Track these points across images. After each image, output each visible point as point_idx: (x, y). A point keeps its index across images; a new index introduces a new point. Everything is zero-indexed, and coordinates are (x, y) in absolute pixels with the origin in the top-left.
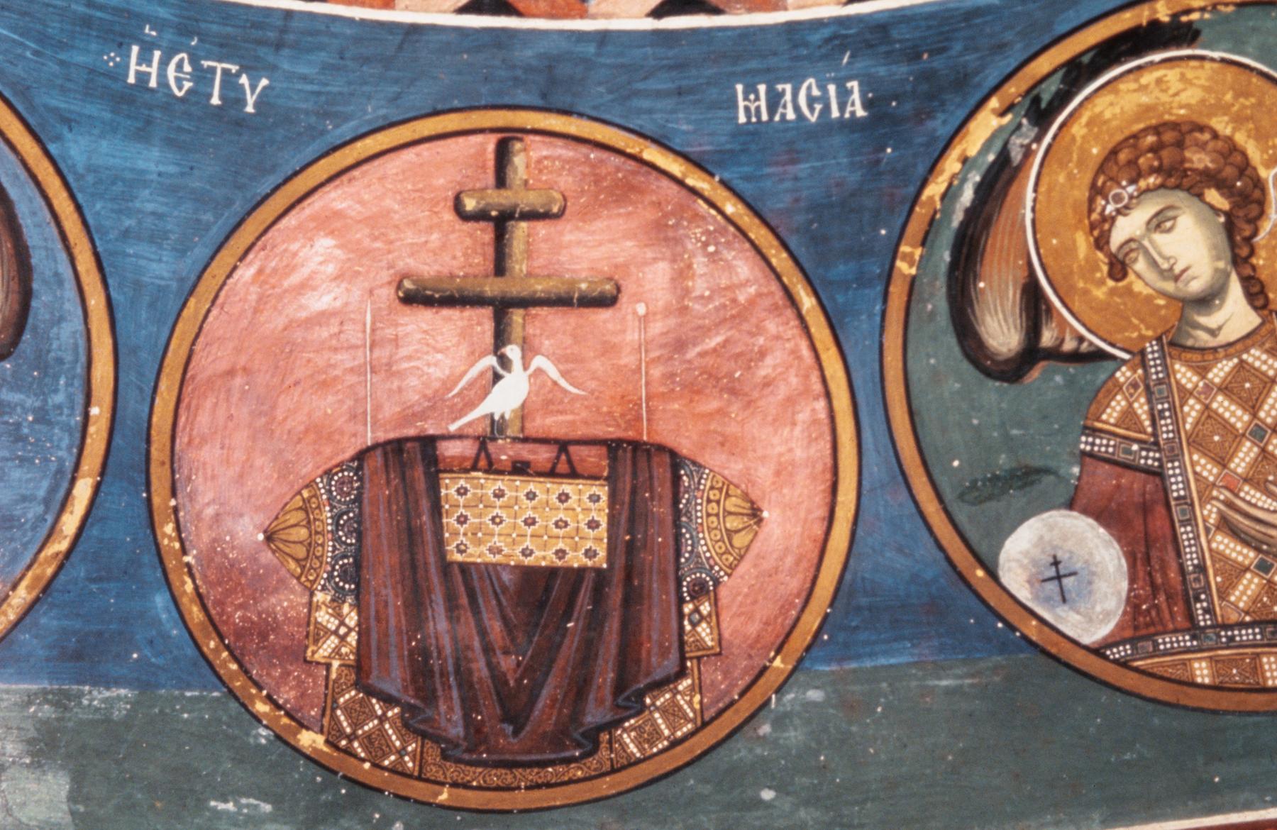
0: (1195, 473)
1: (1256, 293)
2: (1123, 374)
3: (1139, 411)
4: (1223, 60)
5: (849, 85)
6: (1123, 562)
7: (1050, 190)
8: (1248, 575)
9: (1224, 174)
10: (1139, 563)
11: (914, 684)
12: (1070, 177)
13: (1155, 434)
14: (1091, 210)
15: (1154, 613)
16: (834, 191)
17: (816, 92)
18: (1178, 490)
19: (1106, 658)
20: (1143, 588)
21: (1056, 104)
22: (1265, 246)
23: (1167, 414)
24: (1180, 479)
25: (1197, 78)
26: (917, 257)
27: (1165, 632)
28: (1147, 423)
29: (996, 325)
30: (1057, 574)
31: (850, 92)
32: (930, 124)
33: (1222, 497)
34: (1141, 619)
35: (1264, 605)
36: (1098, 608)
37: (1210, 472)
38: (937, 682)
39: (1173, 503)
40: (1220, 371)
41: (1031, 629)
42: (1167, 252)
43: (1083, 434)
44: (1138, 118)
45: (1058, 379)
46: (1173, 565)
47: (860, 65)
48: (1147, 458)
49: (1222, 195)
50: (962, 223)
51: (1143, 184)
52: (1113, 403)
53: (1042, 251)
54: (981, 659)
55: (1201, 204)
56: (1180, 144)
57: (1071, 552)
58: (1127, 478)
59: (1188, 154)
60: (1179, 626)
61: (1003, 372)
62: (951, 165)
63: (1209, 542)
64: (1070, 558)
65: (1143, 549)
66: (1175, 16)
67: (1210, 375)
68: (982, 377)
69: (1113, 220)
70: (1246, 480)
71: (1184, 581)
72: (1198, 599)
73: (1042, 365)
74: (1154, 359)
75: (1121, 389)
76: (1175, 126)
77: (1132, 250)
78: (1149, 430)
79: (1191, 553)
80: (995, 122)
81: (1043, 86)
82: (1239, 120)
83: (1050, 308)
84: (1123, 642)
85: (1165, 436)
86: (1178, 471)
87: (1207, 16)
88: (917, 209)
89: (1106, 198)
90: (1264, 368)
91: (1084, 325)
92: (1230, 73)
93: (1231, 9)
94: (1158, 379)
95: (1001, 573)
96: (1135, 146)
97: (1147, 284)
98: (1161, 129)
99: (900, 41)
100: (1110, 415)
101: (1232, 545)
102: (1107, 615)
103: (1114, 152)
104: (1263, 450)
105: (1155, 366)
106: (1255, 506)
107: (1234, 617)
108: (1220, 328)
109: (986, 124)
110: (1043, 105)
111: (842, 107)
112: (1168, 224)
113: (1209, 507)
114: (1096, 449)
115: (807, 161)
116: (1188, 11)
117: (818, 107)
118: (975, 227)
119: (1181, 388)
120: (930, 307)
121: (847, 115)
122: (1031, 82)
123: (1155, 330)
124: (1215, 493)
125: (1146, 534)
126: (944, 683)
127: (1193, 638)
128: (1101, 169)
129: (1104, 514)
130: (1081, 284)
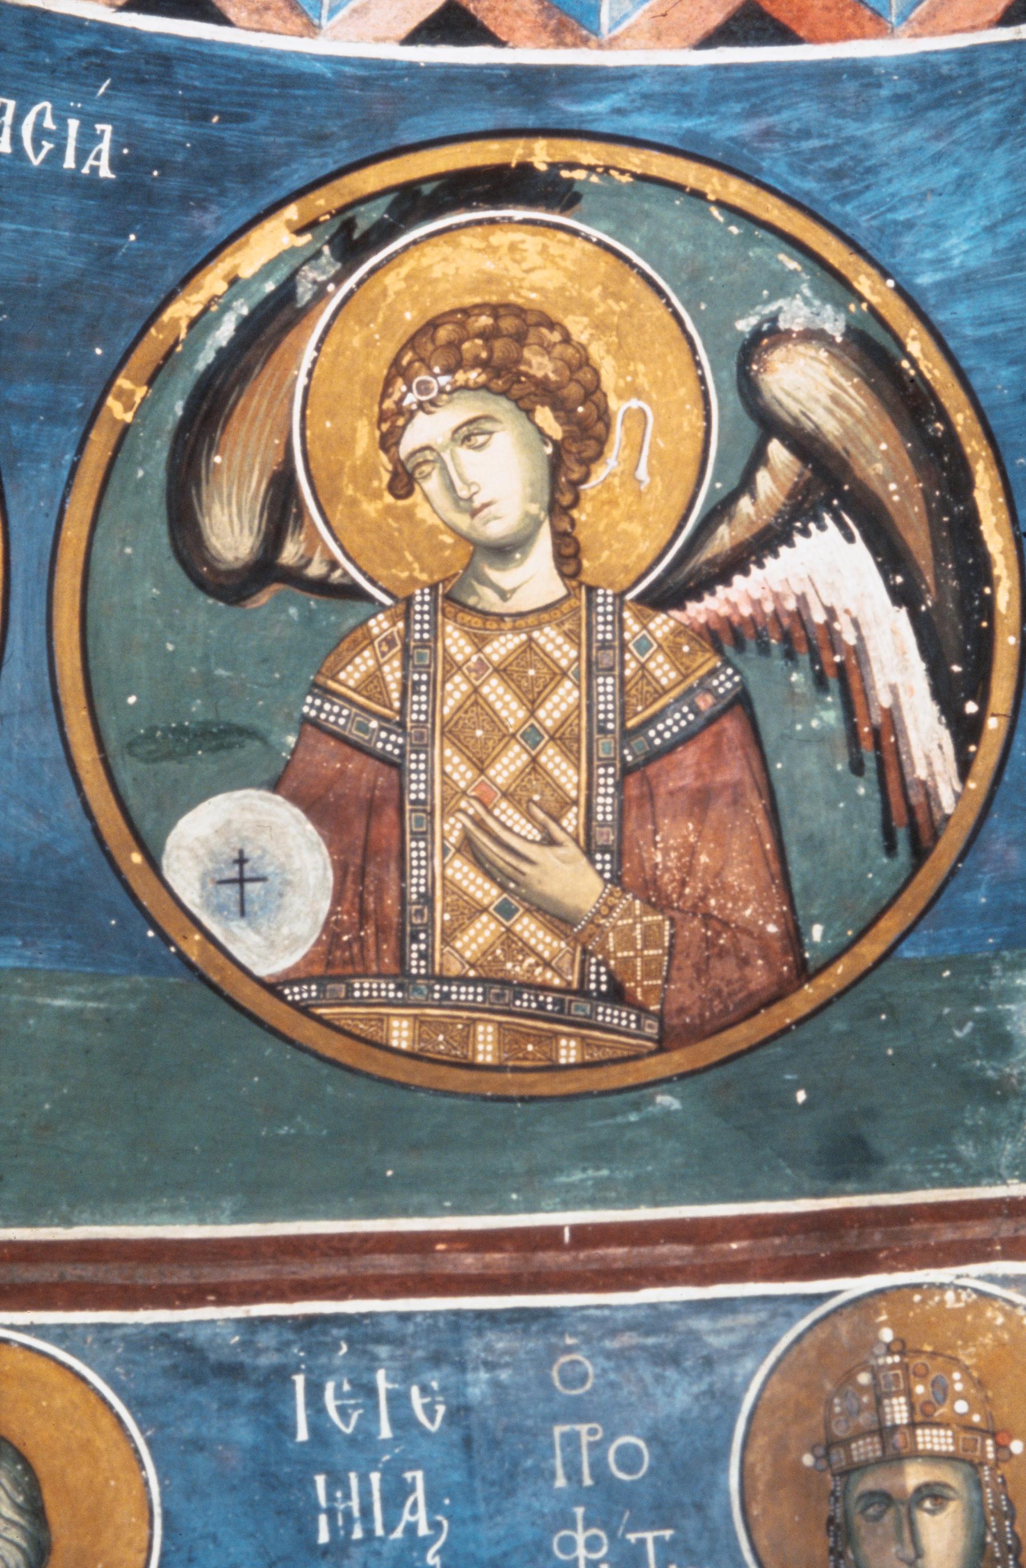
0: (443, 773)
1: (568, 556)
2: (379, 624)
3: (389, 678)
4: (600, 243)
5: (99, 127)
6: (330, 874)
7: (337, 353)
8: (484, 918)
9: (565, 392)
10: (350, 878)
11: (16, 998)
12: (369, 343)
13: (402, 712)
14: (385, 395)
15: (356, 949)
16: (45, 273)
17: (49, 123)
18: (417, 792)
19: (282, 998)
20: (348, 913)
21: (373, 237)
22: (593, 498)
23: (423, 688)
24: (423, 777)
25: (562, 257)
26: (138, 400)
27: (365, 975)
28: (395, 695)
29: (226, 519)
30: (240, 877)
31: (100, 138)
32: (197, 218)
33: (471, 811)
34: (338, 953)
35: (496, 959)
36: (285, 930)
37: (463, 775)
38: (48, 1001)
39: (408, 807)
40: (502, 646)
41: (193, 947)
42: (470, 475)
43: (311, 693)
44: (473, 291)
45: (293, 611)
46: (393, 891)
47: (123, 103)
48: (386, 741)
49: (557, 418)
50: (209, 367)
51: (460, 377)
52: (358, 660)
53: (308, 433)
54: (116, 976)
55: (529, 426)
56: (520, 338)
57: (265, 851)
58: (355, 763)
59: (527, 353)
60: (384, 969)
61: (221, 586)
62: (213, 282)
63: (444, 867)
64: (261, 858)
65: (358, 861)
66: (554, 166)
67: (488, 650)
68: (192, 586)
69: (412, 414)
70: (505, 795)
71: (403, 913)
72: (415, 939)
73: (276, 587)
74: (422, 613)
75: (372, 643)
76: (519, 311)
77: (426, 462)
78: (397, 705)
79: (419, 877)
80: (287, 240)
81: (362, 209)
82: (600, 326)
83: (302, 512)
84: (309, 980)
85: (414, 717)
86: (422, 766)
87: (594, 179)
88: (153, 331)
89: (409, 384)
90: (557, 654)
91: (341, 547)
92: (605, 263)
93: (626, 179)
94: (422, 639)
95: (165, 862)
96: (462, 325)
97: (435, 511)
98: (502, 311)
99: (185, 87)
100: (350, 675)
101: (472, 876)
102: (296, 940)
103: (433, 325)
104: (534, 760)
105: (422, 622)
106: (510, 829)
107: (455, 968)
108: (514, 591)
109: (273, 239)
110: (356, 235)
111: (81, 156)
112: (481, 439)
113: (452, 820)
114: (323, 716)
115: (13, 220)
116: (572, 166)
117: (47, 146)
118: (227, 377)
119: (448, 659)
120: (140, 473)
121: (86, 170)
122: (348, 199)
123: (431, 574)
124: (463, 804)
125: (366, 841)
126: (59, 1003)
127: (399, 987)
128: (411, 343)
129: (319, 807)
130: (350, 491)
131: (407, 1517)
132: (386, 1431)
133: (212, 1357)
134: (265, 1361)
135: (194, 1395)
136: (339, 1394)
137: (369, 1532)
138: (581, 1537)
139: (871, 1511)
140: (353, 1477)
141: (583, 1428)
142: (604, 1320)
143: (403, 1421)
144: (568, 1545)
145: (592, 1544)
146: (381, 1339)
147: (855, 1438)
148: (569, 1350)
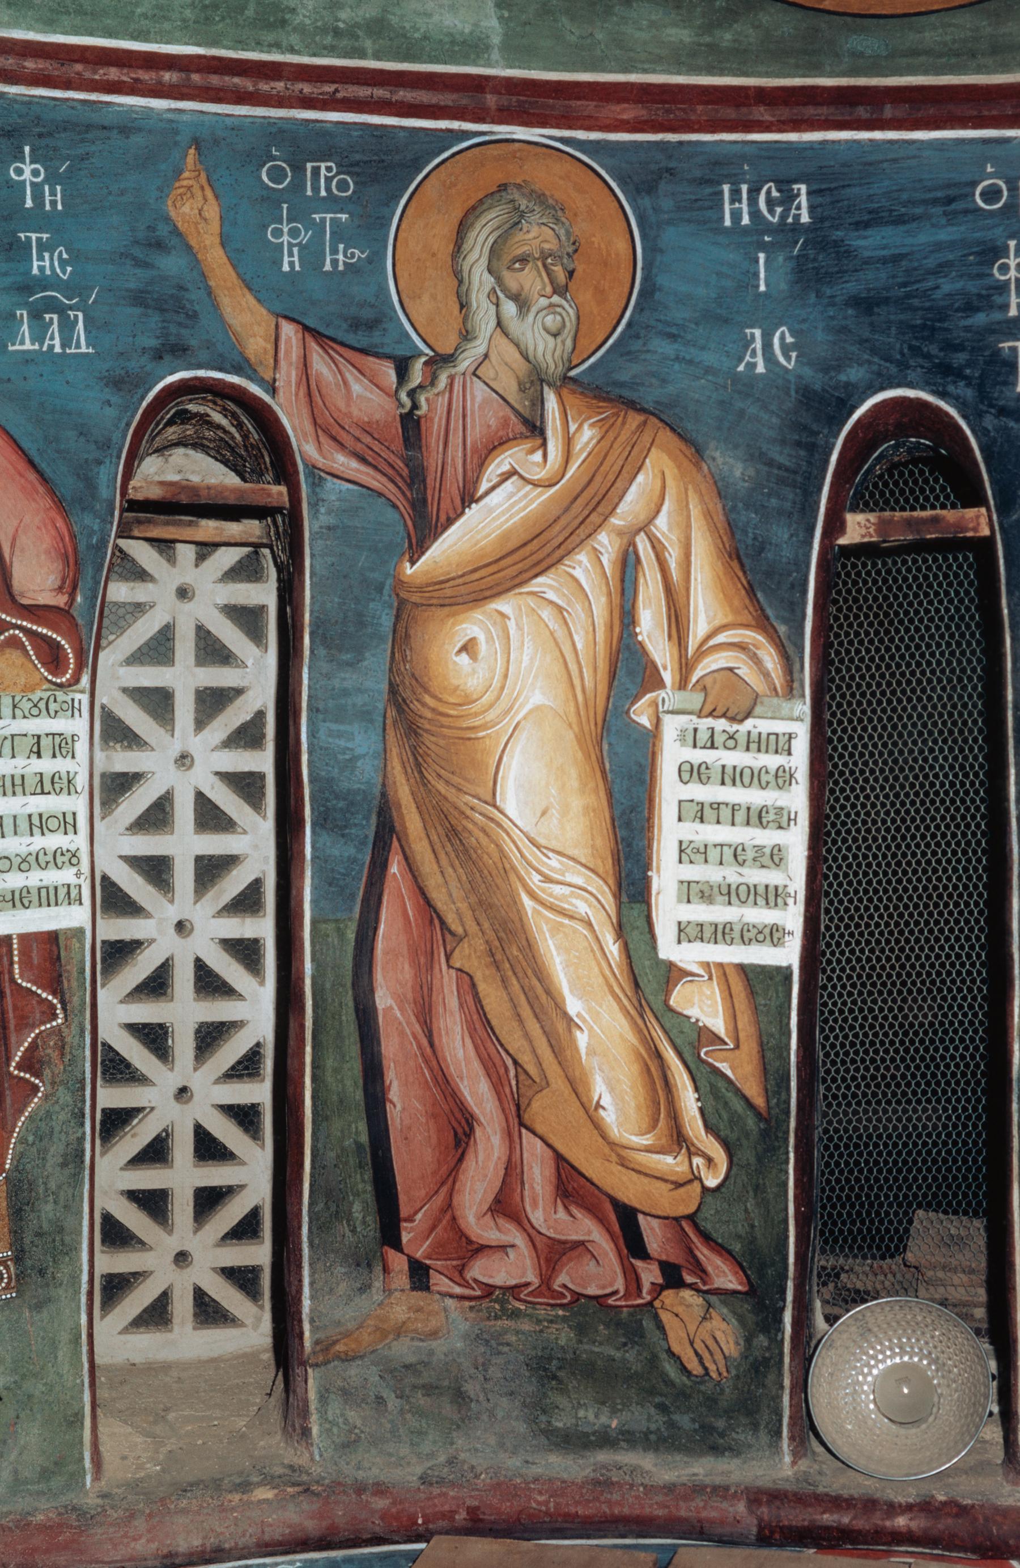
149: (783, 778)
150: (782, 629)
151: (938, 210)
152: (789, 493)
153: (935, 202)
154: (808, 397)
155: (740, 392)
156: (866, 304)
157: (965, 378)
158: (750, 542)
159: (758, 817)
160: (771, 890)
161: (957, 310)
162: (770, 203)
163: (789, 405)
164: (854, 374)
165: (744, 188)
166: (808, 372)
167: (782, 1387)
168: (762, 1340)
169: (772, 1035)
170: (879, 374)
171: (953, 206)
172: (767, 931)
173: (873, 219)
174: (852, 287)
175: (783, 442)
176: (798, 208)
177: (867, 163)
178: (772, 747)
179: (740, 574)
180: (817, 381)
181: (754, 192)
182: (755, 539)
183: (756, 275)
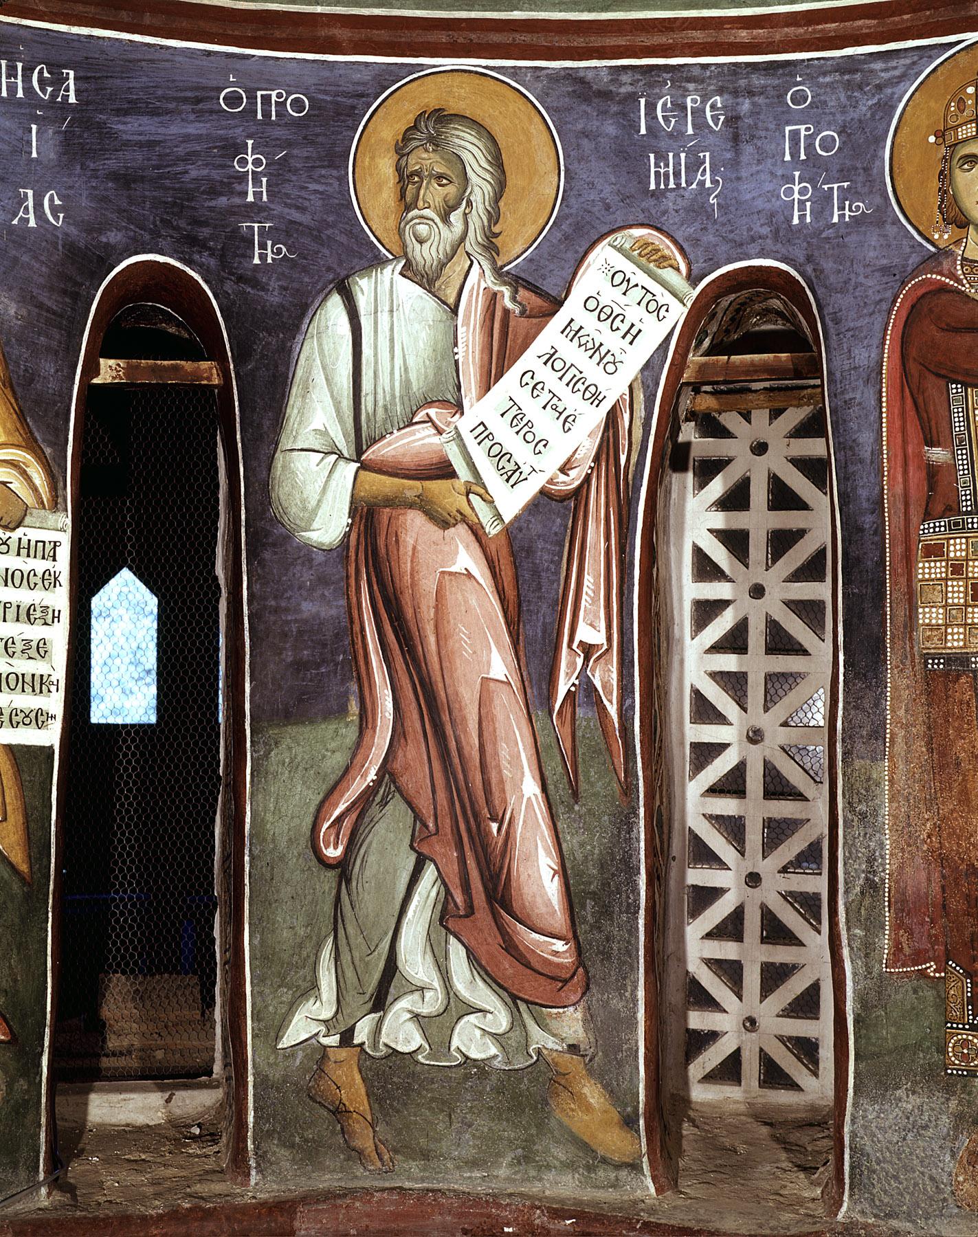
131: (699, 176)
132: (690, 131)
133: (595, 87)
134: (623, 90)
135: (584, 107)
136: (664, 108)
137: (678, 185)
138: (796, 188)
139: (966, 166)
140: (671, 155)
141: (803, 127)
142: (821, 66)
143: (700, 125)
144: (790, 192)
145: (803, 192)
146: (689, 80)
147: (960, 125)
148: (799, 84)
149: (49, 580)
150: (48, 451)
151: (188, 107)
152: (55, 333)
153: (185, 100)
154: (73, 252)
155: (14, 242)
156: (125, 180)
157: (210, 249)
158: (22, 373)
159: (28, 615)
160: (37, 679)
161: (202, 193)
162: (42, 81)
163: (55, 258)
164: (114, 237)
165: (20, 65)
166: (73, 230)
167: (40, 1126)
168: (22, 1084)
169: (36, 808)
170: (134, 239)
171: (200, 106)
172: (33, 715)
173: (132, 108)
174: (111, 164)
175: (52, 289)
176: (67, 90)
177: (132, 58)
178: (40, 554)
179: (13, 401)
180: (82, 241)
181: (28, 71)
182: (26, 370)
183: (29, 143)
